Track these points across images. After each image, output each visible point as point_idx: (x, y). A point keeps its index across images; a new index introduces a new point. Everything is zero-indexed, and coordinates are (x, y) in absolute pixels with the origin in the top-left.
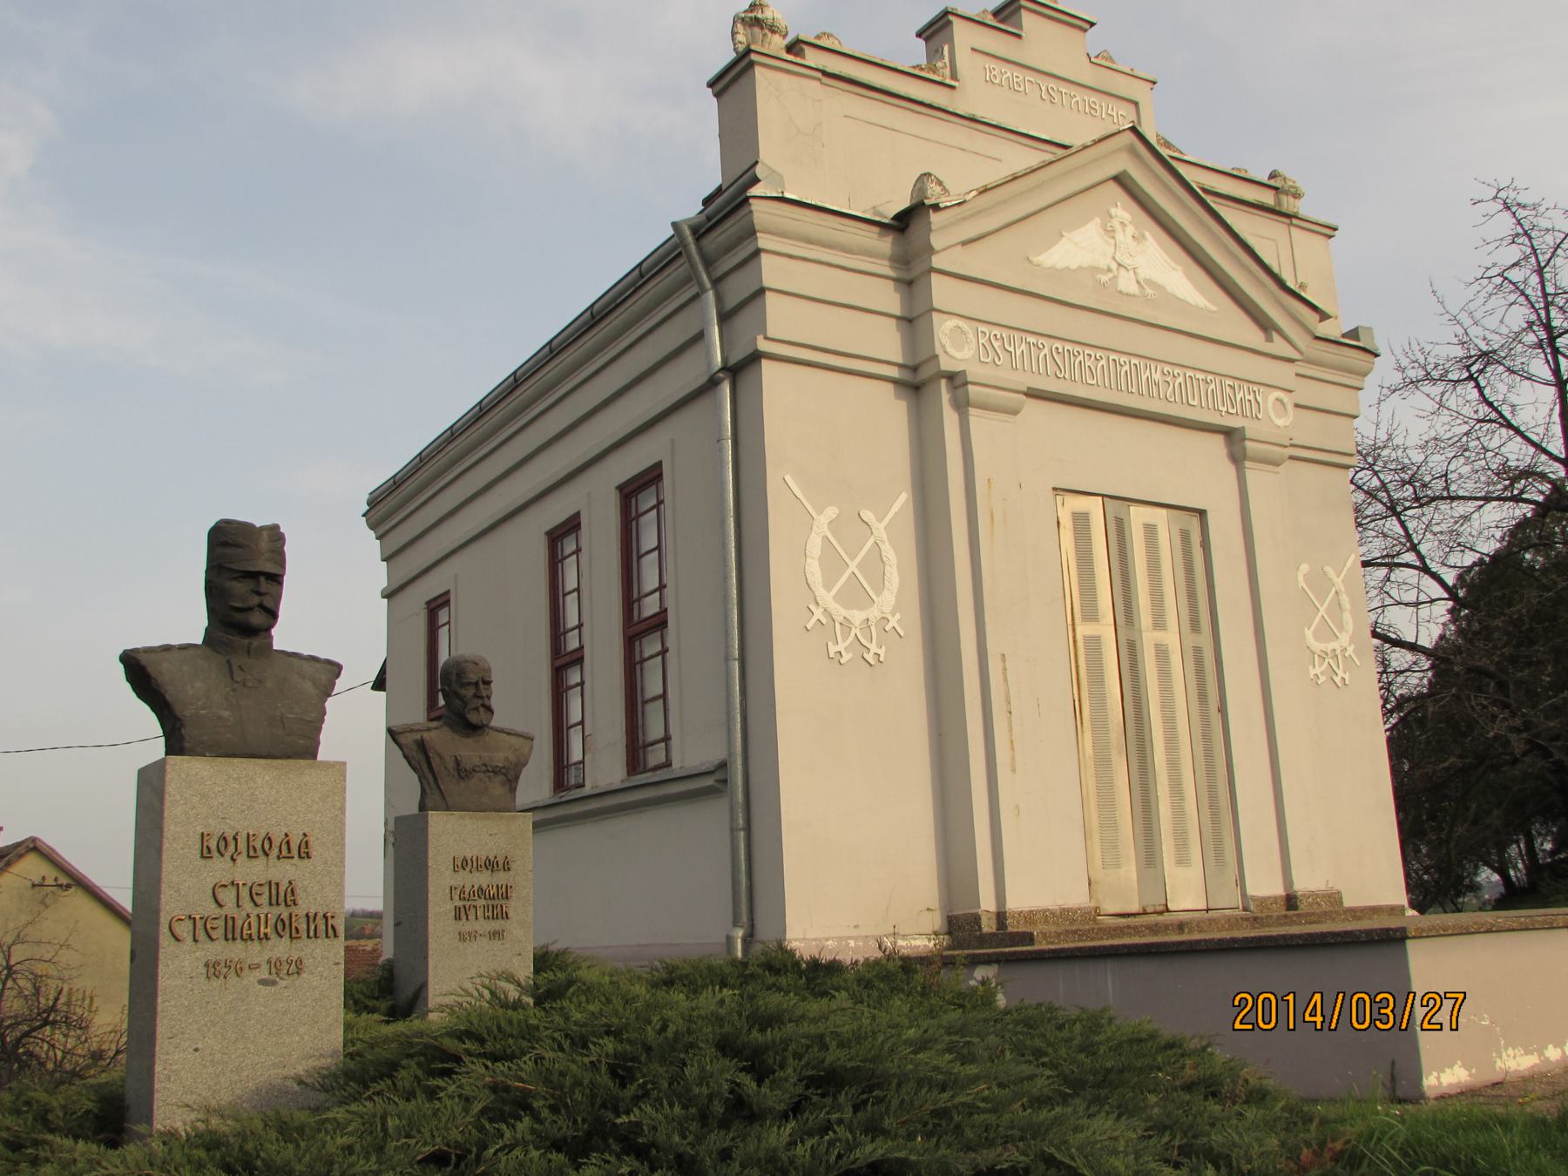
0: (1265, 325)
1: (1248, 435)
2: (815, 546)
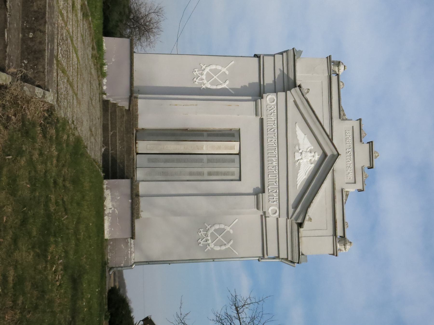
0: (295, 207)
1: (263, 194)
2: (219, 67)
